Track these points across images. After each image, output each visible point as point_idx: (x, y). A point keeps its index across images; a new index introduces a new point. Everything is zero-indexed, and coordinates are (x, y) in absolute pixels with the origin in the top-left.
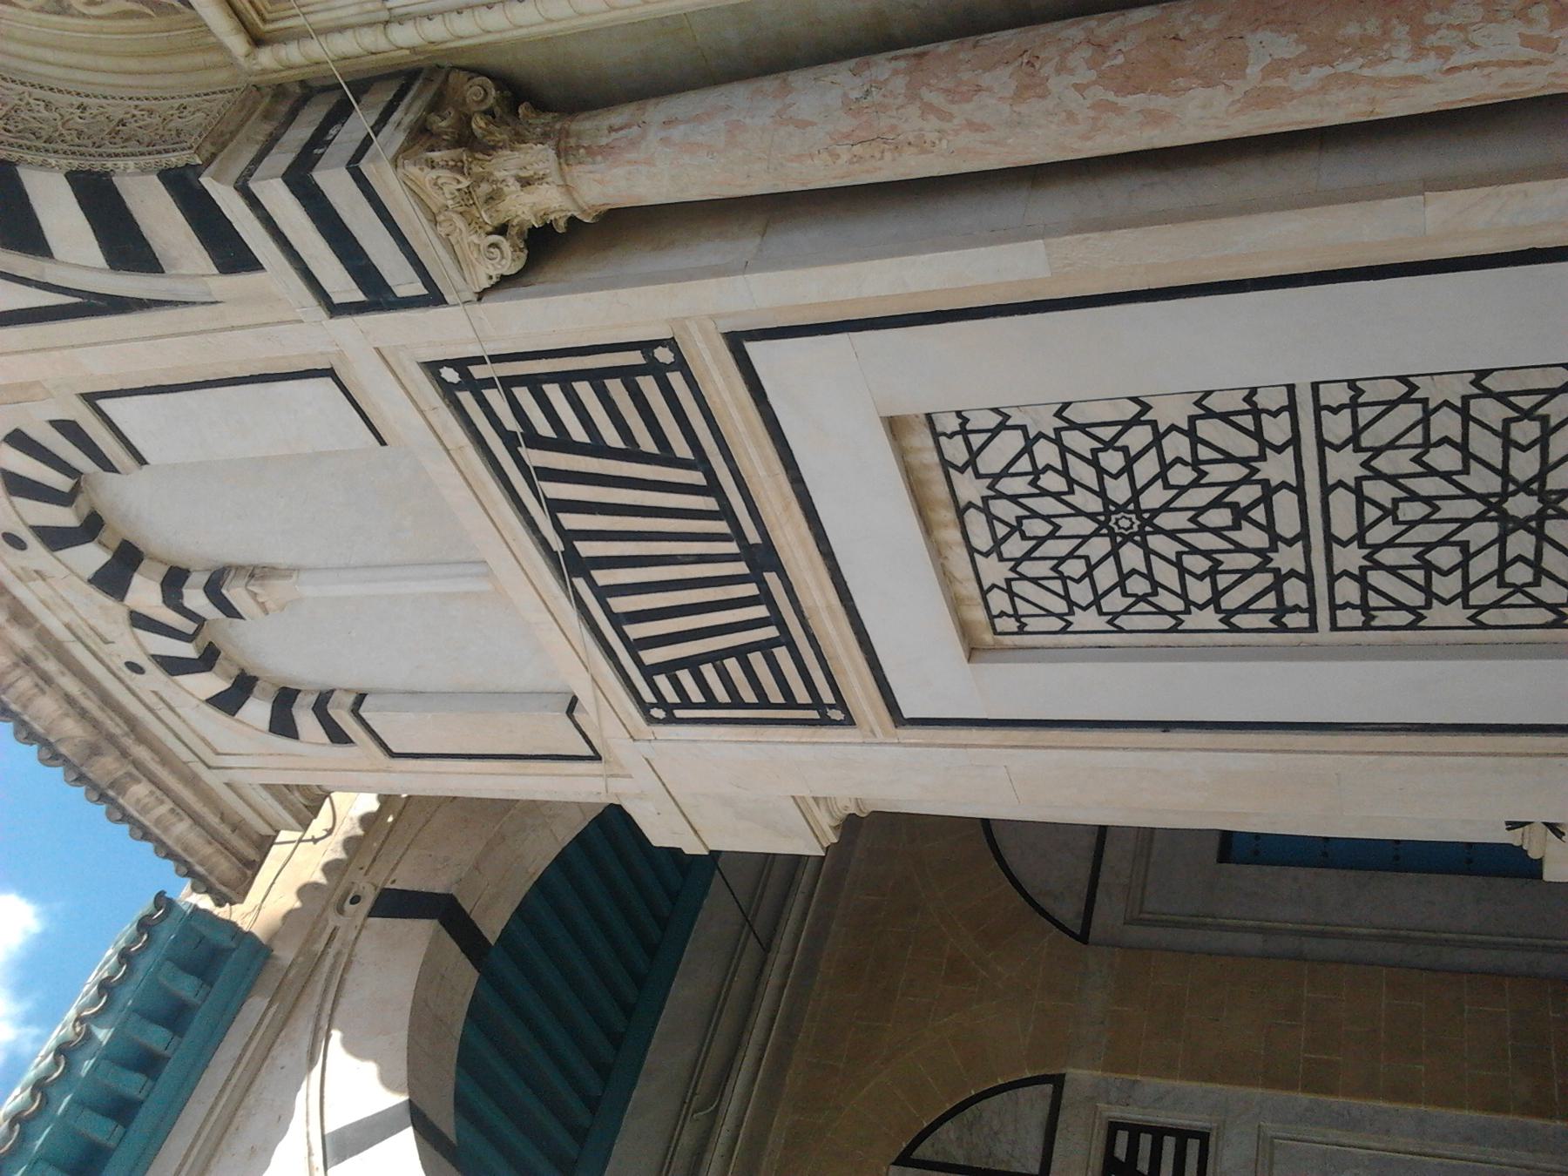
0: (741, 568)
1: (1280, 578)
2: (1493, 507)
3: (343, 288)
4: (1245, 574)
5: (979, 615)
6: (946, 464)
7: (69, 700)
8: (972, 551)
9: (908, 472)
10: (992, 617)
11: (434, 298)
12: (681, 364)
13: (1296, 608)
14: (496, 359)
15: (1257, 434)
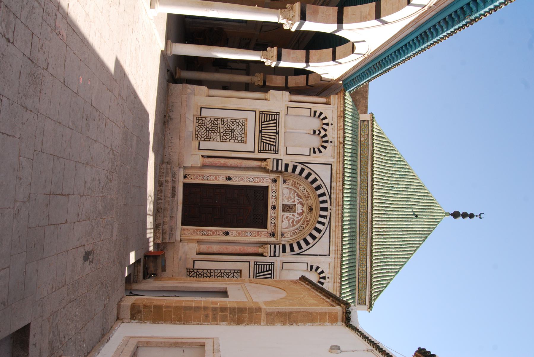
0: (263, 131)
1: (223, 124)
2: (209, 130)
3: (280, 161)
4: (225, 125)
5: (246, 122)
11: (273, 159)
12: (259, 150)
14: (271, 153)
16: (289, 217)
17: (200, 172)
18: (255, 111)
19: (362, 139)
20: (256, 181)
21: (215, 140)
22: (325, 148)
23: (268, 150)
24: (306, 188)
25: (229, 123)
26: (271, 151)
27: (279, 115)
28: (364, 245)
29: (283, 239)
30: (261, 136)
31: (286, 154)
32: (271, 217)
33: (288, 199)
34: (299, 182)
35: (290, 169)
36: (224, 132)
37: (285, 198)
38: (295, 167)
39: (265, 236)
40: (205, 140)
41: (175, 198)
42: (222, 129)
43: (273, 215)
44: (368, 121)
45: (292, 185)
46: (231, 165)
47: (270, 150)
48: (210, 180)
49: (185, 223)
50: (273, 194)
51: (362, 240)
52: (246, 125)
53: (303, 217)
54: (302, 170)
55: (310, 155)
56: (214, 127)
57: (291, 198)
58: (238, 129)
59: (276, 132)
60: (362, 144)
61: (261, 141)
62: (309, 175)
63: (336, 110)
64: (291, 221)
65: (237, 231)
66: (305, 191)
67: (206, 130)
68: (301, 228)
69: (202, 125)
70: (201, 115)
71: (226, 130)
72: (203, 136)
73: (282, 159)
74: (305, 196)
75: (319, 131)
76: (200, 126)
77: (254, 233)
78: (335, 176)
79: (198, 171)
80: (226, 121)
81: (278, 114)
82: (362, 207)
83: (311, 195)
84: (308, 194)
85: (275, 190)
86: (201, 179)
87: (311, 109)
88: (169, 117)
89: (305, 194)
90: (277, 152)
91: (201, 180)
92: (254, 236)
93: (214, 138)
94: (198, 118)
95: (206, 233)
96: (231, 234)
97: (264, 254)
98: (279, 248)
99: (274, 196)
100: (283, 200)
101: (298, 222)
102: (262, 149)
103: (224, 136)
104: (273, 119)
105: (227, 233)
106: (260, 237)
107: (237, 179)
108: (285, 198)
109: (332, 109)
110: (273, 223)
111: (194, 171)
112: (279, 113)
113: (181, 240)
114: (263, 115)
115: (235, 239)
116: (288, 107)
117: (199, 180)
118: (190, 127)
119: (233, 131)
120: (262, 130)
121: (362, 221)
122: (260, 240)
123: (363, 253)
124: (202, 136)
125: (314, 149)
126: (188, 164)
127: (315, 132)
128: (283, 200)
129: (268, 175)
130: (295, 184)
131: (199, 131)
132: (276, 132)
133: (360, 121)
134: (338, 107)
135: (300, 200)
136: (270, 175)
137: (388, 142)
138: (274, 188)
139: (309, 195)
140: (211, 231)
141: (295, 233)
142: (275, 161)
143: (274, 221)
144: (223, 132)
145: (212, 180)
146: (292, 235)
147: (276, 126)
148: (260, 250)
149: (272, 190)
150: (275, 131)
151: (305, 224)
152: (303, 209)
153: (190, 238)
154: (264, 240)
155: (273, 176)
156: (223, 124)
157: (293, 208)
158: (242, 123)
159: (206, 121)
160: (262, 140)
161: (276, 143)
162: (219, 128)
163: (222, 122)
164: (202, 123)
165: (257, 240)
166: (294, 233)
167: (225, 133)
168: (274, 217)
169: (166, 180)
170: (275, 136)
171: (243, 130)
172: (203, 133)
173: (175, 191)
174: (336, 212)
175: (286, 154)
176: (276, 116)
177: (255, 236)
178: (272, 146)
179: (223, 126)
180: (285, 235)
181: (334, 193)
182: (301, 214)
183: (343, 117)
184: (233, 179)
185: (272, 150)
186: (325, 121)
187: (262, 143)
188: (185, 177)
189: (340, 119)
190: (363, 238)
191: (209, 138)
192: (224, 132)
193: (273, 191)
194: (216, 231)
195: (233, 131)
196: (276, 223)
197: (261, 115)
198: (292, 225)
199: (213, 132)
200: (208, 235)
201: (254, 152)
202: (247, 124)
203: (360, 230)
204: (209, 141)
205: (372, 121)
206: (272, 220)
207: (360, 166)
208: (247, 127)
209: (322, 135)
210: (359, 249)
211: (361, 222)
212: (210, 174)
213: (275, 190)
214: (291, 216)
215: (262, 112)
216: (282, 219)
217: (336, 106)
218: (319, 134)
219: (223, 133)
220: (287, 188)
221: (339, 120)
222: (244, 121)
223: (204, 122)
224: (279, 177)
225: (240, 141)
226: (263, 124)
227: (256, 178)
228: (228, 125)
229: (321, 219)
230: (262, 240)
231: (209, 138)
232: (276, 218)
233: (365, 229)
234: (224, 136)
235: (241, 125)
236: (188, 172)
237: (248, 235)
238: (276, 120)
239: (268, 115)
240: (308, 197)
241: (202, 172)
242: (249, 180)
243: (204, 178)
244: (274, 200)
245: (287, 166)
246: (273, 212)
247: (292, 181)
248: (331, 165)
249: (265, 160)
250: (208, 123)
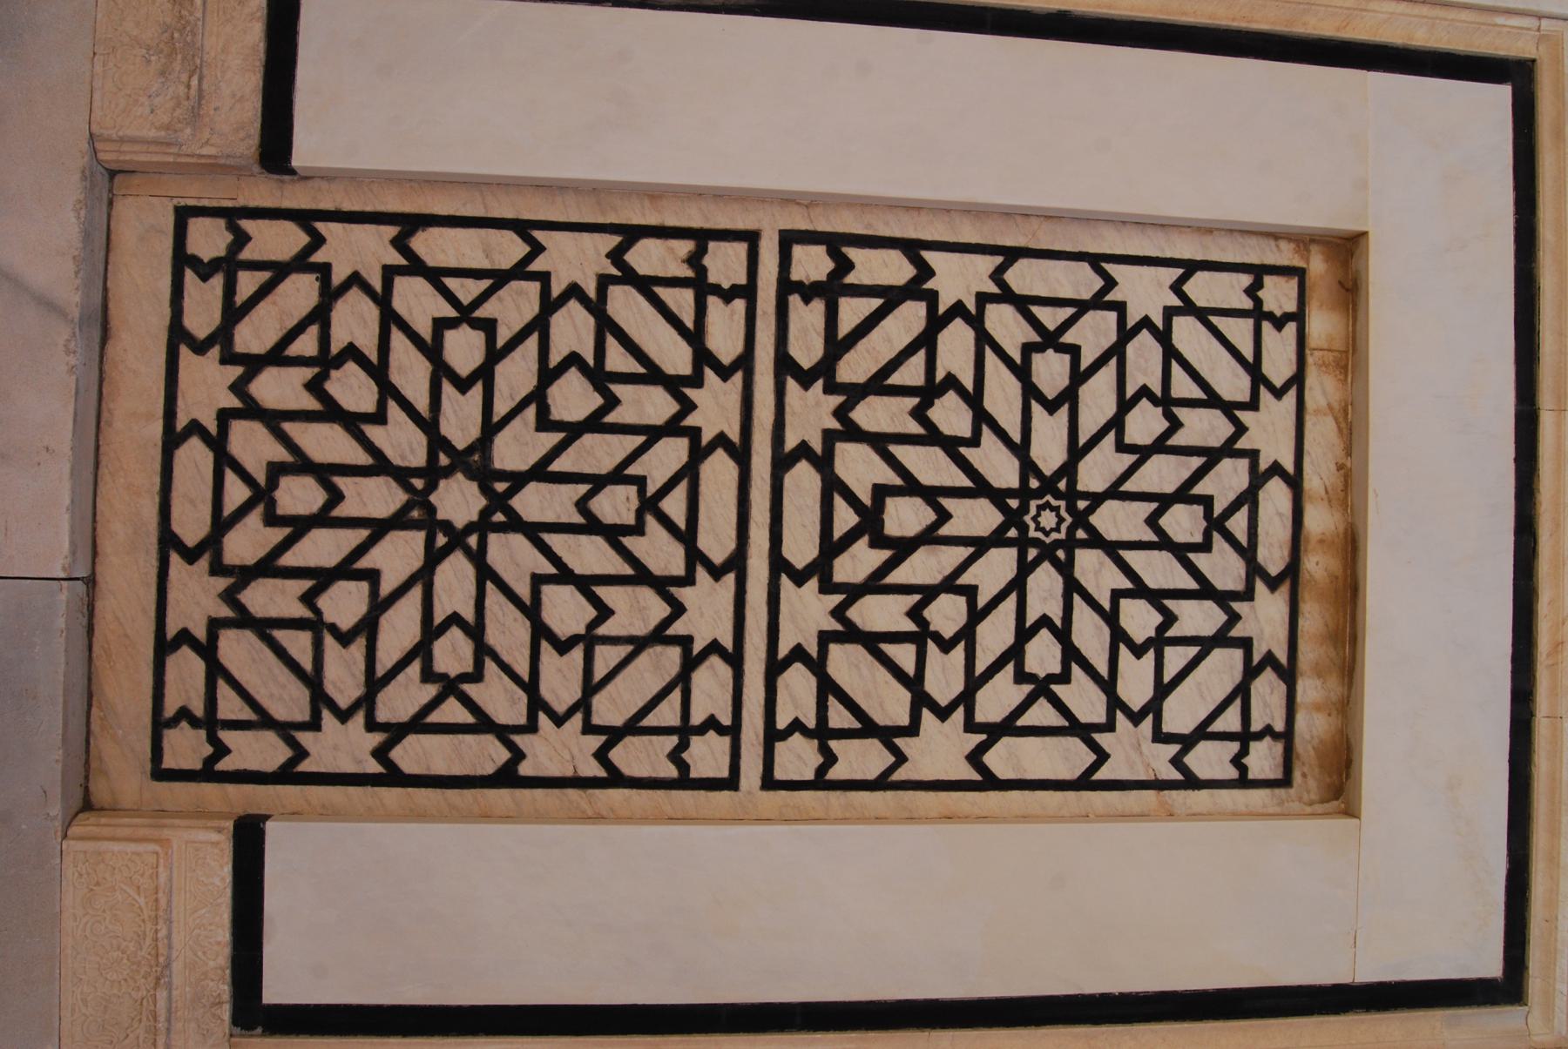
1: (825, 371)
4: (878, 385)
5: (1322, 325)
6: (1289, 675)
8: (1295, 482)
9: (1349, 669)
10: (1299, 317)
13: (809, 292)
15: (827, 688)
21: (629, 758)
25: (956, 348)
36: (858, 562)
42: (803, 481)
52: (1321, 388)
56: (598, 453)
58: (1163, 474)
69: (331, 412)
71: (905, 517)
76: (274, 420)
80: (892, 297)
93: (611, 708)
103: (847, 664)
119: (1047, 521)
124: (313, 681)
144: (831, 548)
156: (825, 371)
158: (1239, 332)
162: (719, 471)
163: (807, 320)
164: (326, 362)
167: (875, 584)
192: (858, 562)
199: (590, 555)
204: (507, 777)
219: (821, 570)
222: (1279, 295)
228: (929, 392)
234: (847, 664)
235: (1232, 383)
250: (464, 349)
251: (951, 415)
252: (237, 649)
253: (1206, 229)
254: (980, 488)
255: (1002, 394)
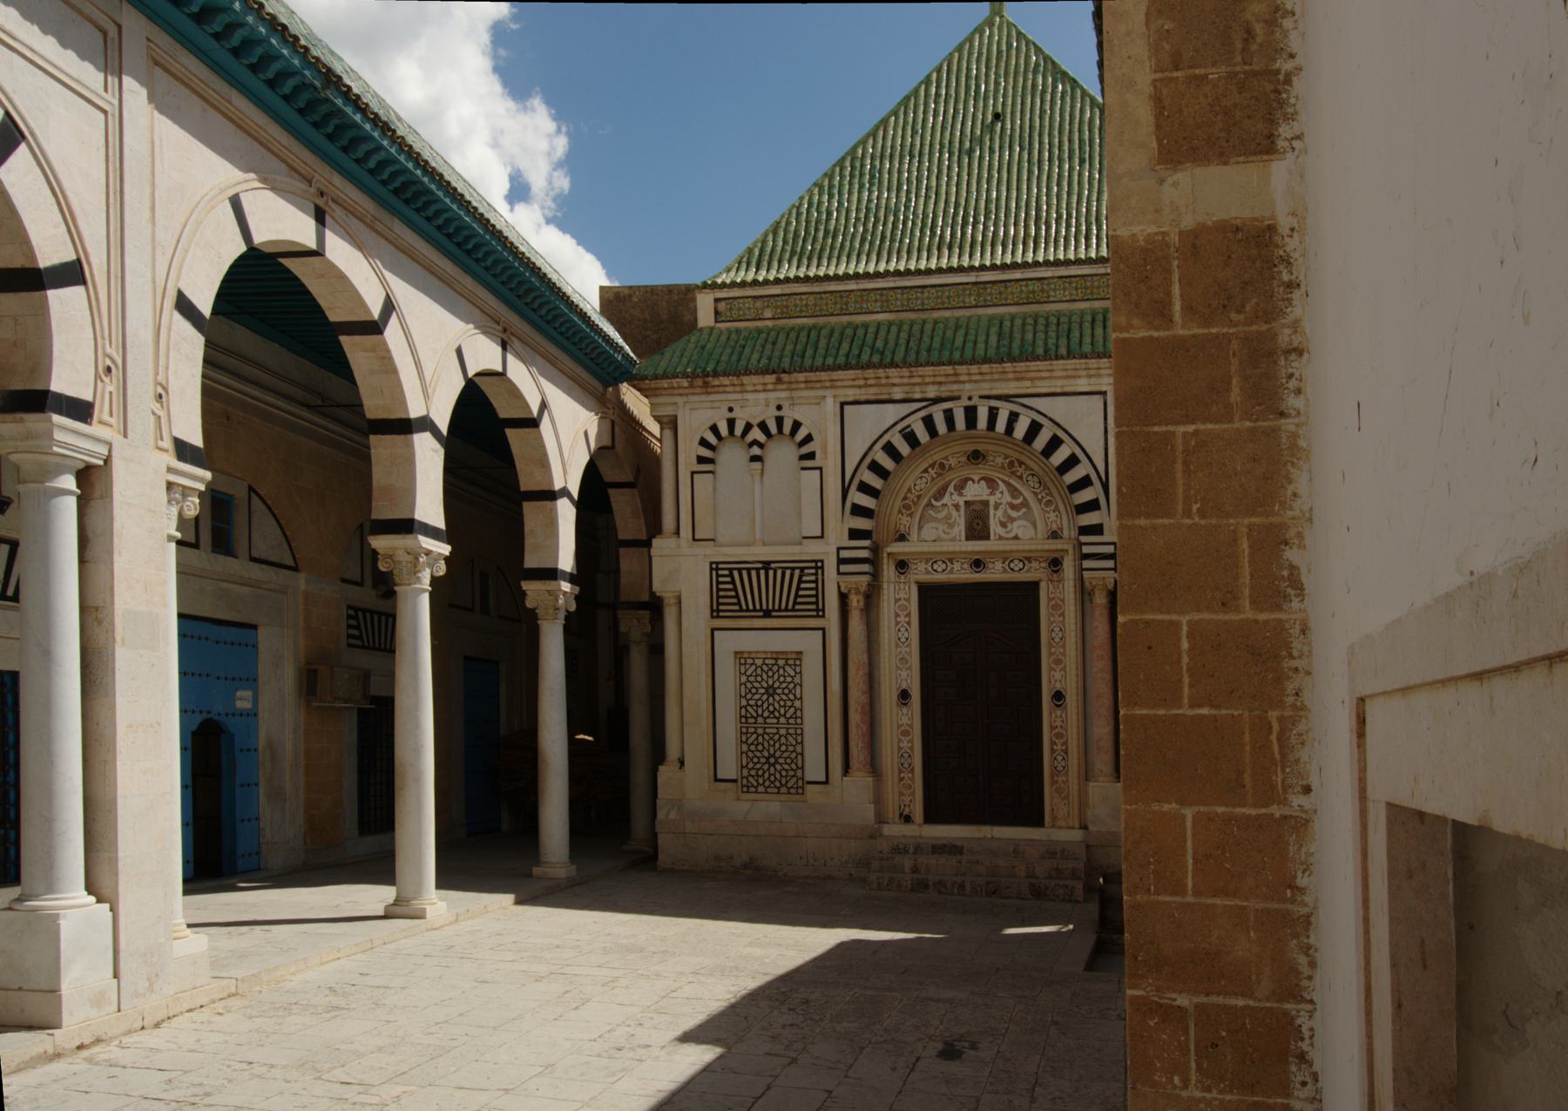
0: (764, 607)
1: (756, 718)
2: (773, 756)
3: (845, 554)
4: (757, 712)
5: (746, 656)
7: (725, 386)
8: (764, 659)
9: (786, 653)
12: (818, 616)
15: (791, 717)
16: (1002, 519)
17: (890, 778)
18: (713, 630)
19: (768, 314)
20: (907, 619)
21: (799, 740)
22: (797, 425)
23: (816, 589)
24: (917, 473)
25: (752, 703)
26: (816, 582)
27: (717, 563)
28: (1074, 285)
29: (1066, 534)
30: (780, 610)
31: (822, 537)
32: (1005, 571)
33: (951, 526)
34: (902, 495)
35: (862, 523)
37: (948, 533)
38: (858, 511)
39: (1061, 586)
40: (800, 765)
41: (963, 847)
42: (768, 721)
43: (999, 565)
44: (717, 300)
45: (911, 515)
46: (864, 693)
47: (813, 585)
48: (912, 748)
49: (1035, 818)
50: (940, 570)
51: (1059, 295)
52: (753, 656)
53: (999, 478)
54: (865, 488)
55: (821, 469)
56: (766, 744)
57: (948, 517)
58: (765, 676)
59: (763, 568)
60: (782, 313)
61: (793, 610)
62: (875, 468)
63: (691, 398)
64: (1014, 514)
65: (1051, 669)
66: (926, 475)
67: (774, 765)
68: (1033, 482)
69: (763, 775)
70: (735, 781)
72: (791, 773)
73: (839, 549)
74: (939, 475)
75: (751, 445)
77: (1052, 619)
78: (872, 390)
79: (890, 783)
80: (747, 711)
81: (715, 567)
82: (964, 302)
83: (936, 458)
84: (932, 466)
85: (926, 563)
86: (910, 775)
87: (693, 473)
88: (745, 866)
89: (935, 476)
90: (819, 564)
91: (913, 774)
92: (1061, 619)
93: (794, 743)
94: (745, 789)
95: (1059, 758)
96: (1058, 686)
97: (1111, 587)
98: (1092, 545)
99: (944, 566)
100: (953, 540)
101: (1014, 492)
102: (814, 607)
104: (728, 579)
105: (1058, 696)
106: (1063, 600)
107: (904, 674)
108: (948, 533)
109: (687, 412)
110: (1021, 565)
111: (890, 795)
112: (711, 563)
113: (1084, 827)
114: (721, 607)
115: (1073, 672)
116: (694, 540)
117: (912, 780)
118: (769, 807)
119: (771, 691)
120: (761, 610)
121: (1003, 296)
122: (1072, 602)
123: (1098, 287)
125: (802, 457)
126: (869, 812)
127: (755, 459)
128: (953, 540)
129: (885, 585)
130: (907, 507)
131: (778, 784)
132: (763, 568)
133: (718, 325)
134: (681, 395)
135: (951, 488)
136: (885, 579)
137: (775, 233)
138: (922, 566)
139: (935, 463)
140: (1055, 744)
141: (1048, 498)
142: (844, 568)
143: (1016, 562)
145: (910, 745)
146: (1052, 508)
147: (749, 570)
148: (1100, 599)
149: (927, 572)
150: (762, 572)
151: (1021, 470)
152: (976, 479)
153: (1076, 800)
154: (1072, 589)
155: (889, 571)
157: (975, 507)
159: (751, 765)
160: (790, 607)
161: (793, 569)
162: (767, 730)
165: (1072, 608)
166: (1049, 503)
168: (1003, 563)
169: (913, 872)
170: (775, 571)
171: (767, 661)
172: (784, 773)
173: (945, 845)
174: (976, 381)
175: (822, 537)
176: (720, 572)
177: (1063, 615)
178: (804, 578)
179: (760, 720)
180: (1054, 527)
181: (922, 392)
182: (991, 483)
183: (706, 379)
184: (904, 686)
185: (813, 578)
186: (724, 431)
187: (797, 607)
188: (907, 819)
189: (713, 386)
190: (1054, 290)
191: (793, 755)
192: (777, 714)
193: (930, 569)
194: (1052, 728)
195: (771, 691)
196: (1021, 556)
197: (721, 614)
198: (1024, 510)
199: (777, 745)
200: (1066, 752)
201: (823, 630)
202: (750, 653)
203: (1032, 303)
204: (802, 754)
205: (715, 288)
206: (1012, 569)
207: (845, 314)
208: (756, 652)
209: (761, 438)
210: (1088, 300)
211: (1006, 299)
212: (896, 751)
213: (926, 563)
214: (1000, 513)
215: (712, 611)
216: (1008, 539)
217: (680, 400)
218: (761, 446)
219: (778, 718)
220: (920, 528)
221: (716, 389)
222: (743, 661)
223: (753, 772)
224: (889, 554)
225: (798, 670)
226: (744, 607)
227: (898, 619)
228: (757, 705)
229: (1001, 426)
230: (1072, 596)
231: (793, 755)
232: (1007, 558)
233: (1026, 286)
235: (753, 667)
236: (892, 811)
237: (1060, 635)
238: (731, 570)
239: (721, 593)
240: (942, 466)
241: (890, 772)
242: (903, 640)
243: (906, 765)
244: (957, 566)
245: (855, 534)
246: (991, 566)
247: (900, 516)
248: (843, 404)
249: (843, 598)
251: (759, 703)
252: (789, 785)
253: (735, 671)
254: (767, 699)
255: (757, 697)
